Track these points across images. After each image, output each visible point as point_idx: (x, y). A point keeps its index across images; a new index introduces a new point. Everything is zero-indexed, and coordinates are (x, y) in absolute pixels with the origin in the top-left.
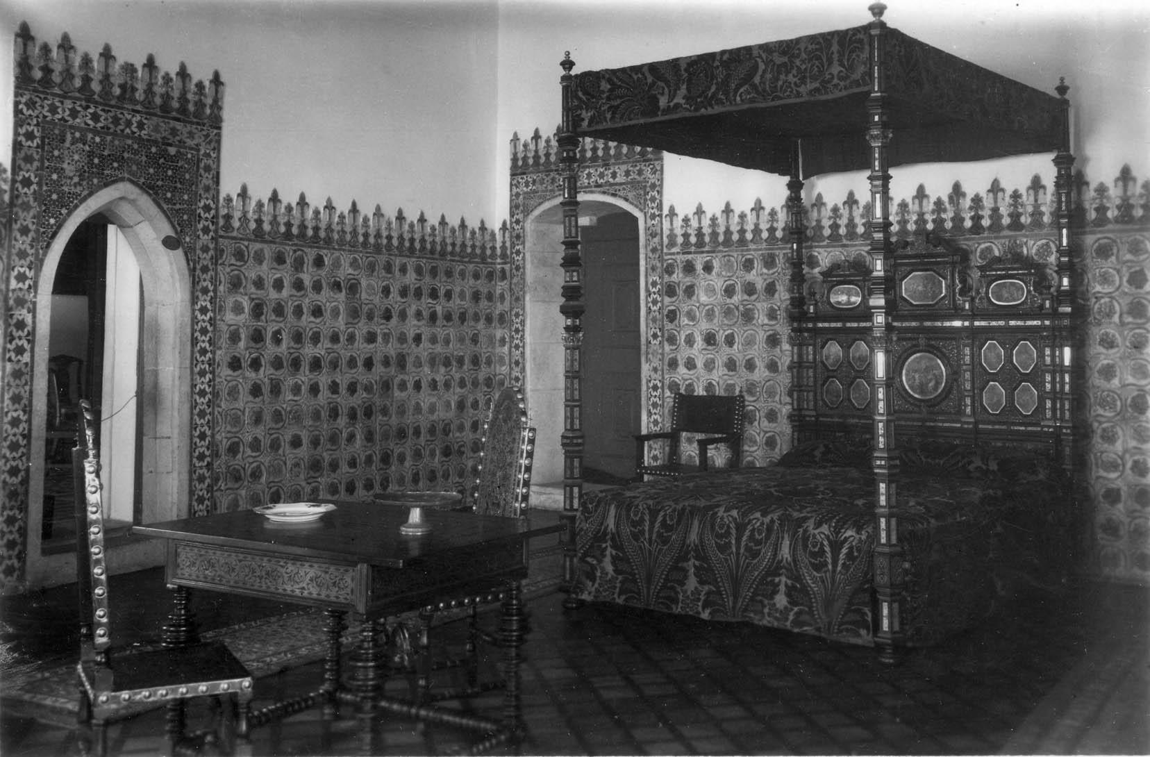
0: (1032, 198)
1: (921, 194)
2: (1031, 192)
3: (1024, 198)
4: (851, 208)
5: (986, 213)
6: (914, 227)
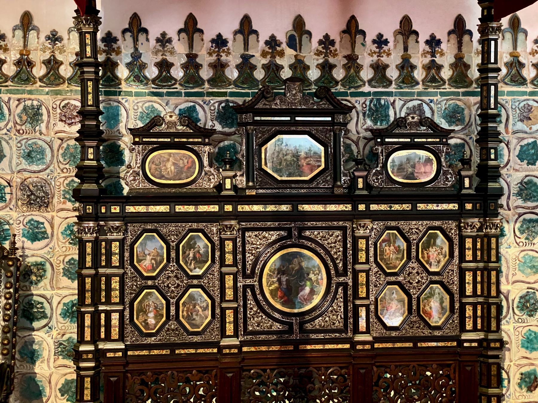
0: (401, 46)
1: (246, 28)
2: (400, 38)
3: (391, 45)
4: (136, 40)
5: (339, 61)
6: (236, 74)
